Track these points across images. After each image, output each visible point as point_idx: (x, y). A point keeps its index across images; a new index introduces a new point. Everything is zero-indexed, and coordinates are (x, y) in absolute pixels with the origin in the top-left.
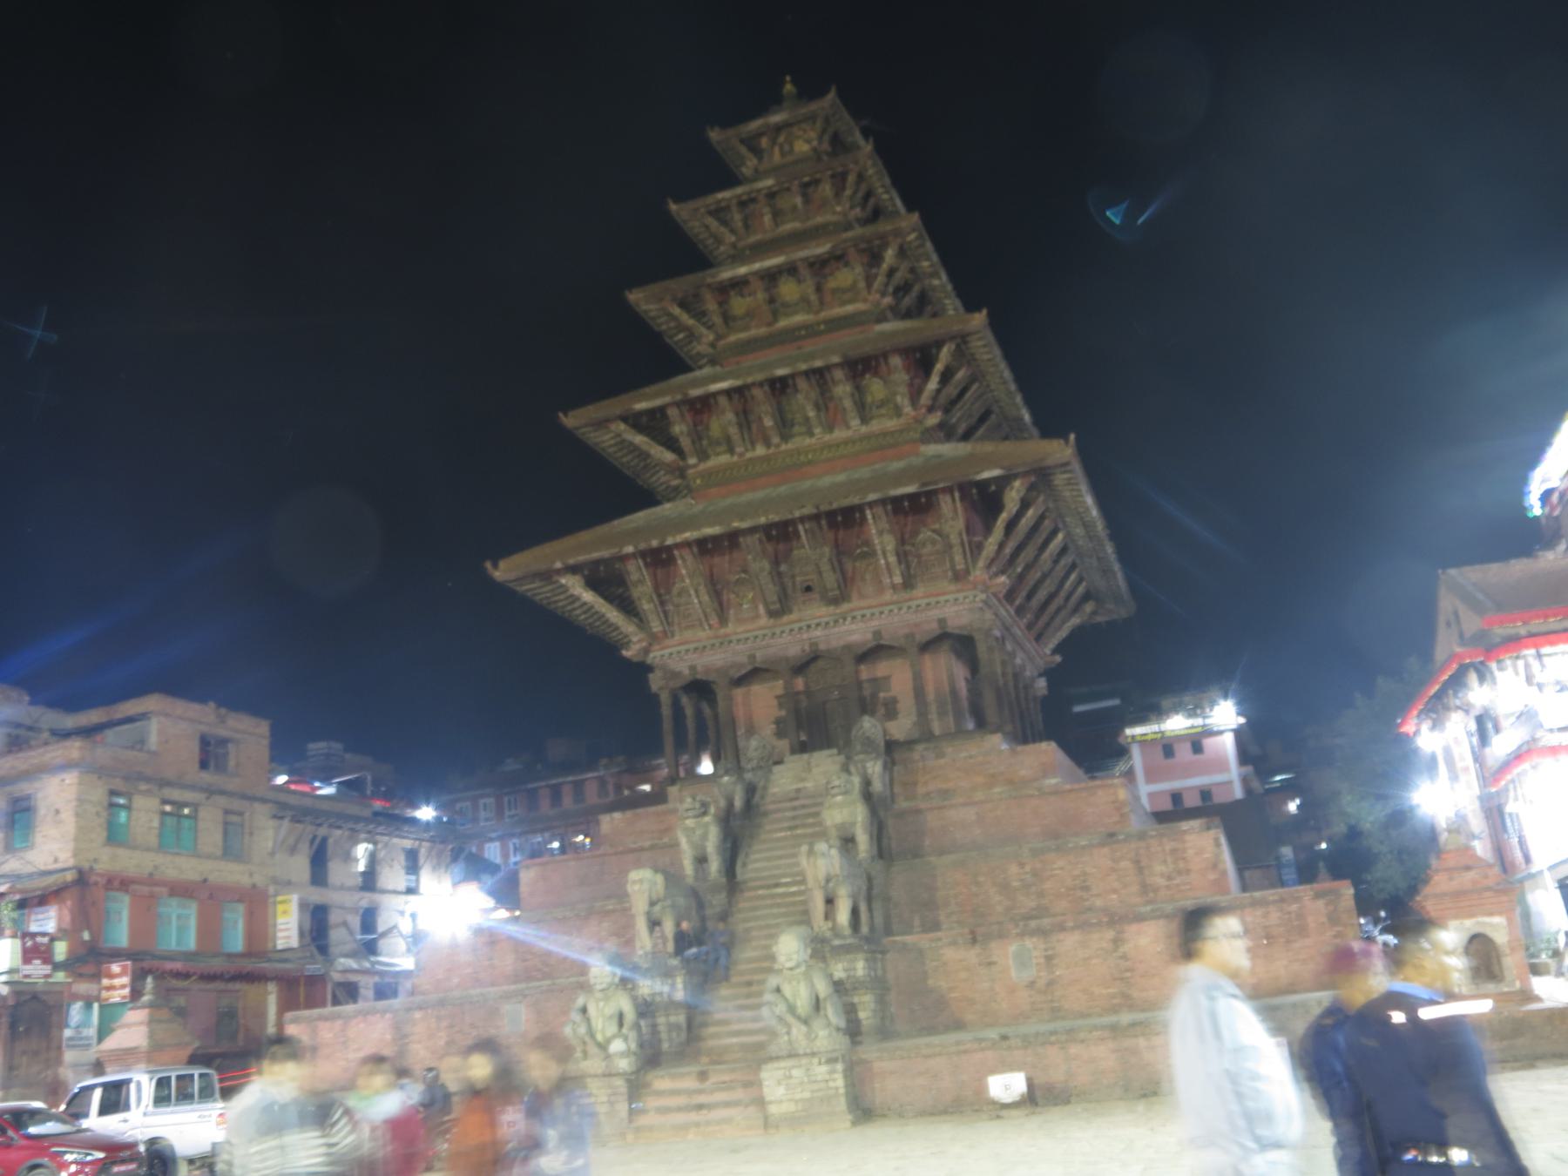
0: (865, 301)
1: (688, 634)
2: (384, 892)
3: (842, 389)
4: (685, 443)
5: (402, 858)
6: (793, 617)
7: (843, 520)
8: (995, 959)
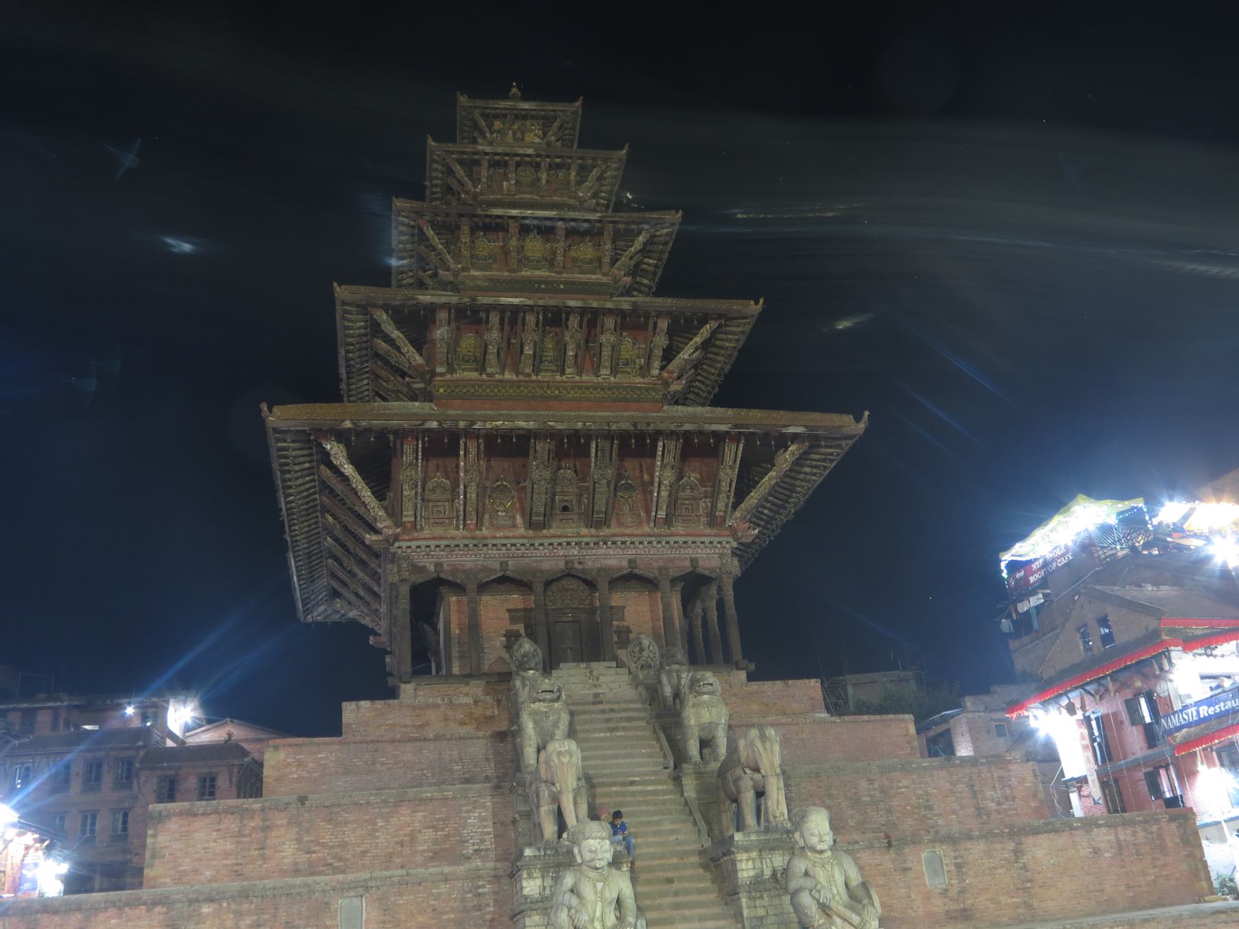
0: (605, 274)
1: (439, 531)
3: (607, 338)
4: (441, 350)
6: (552, 531)
7: (636, 445)
8: (910, 865)
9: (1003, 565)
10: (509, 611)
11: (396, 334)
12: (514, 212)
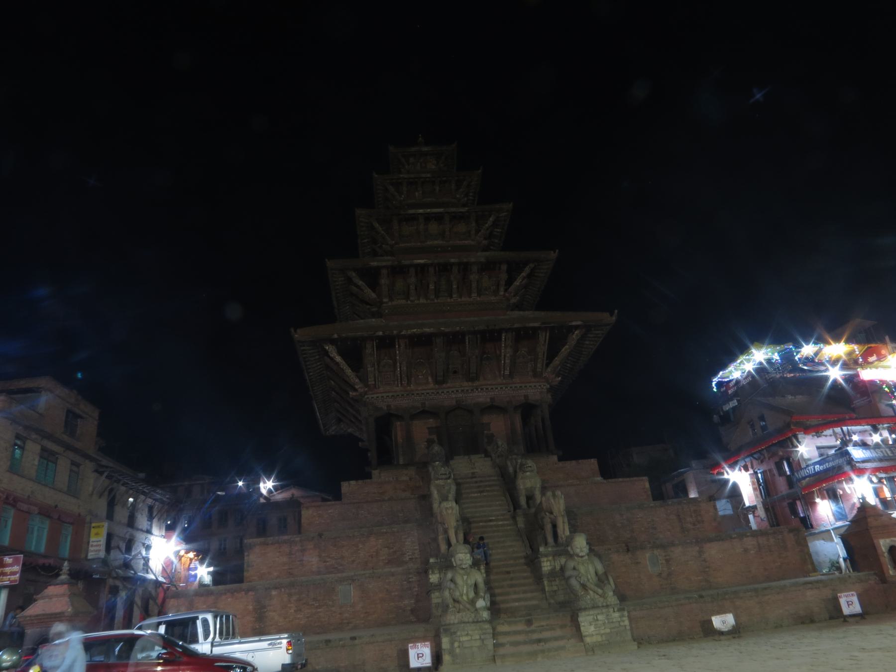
2: (138, 529)
3: (474, 277)
5: (147, 510)
6: (448, 385)
7: (490, 336)
9: (714, 384)
10: (428, 428)
11: (360, 283)
12: (421, 211)
